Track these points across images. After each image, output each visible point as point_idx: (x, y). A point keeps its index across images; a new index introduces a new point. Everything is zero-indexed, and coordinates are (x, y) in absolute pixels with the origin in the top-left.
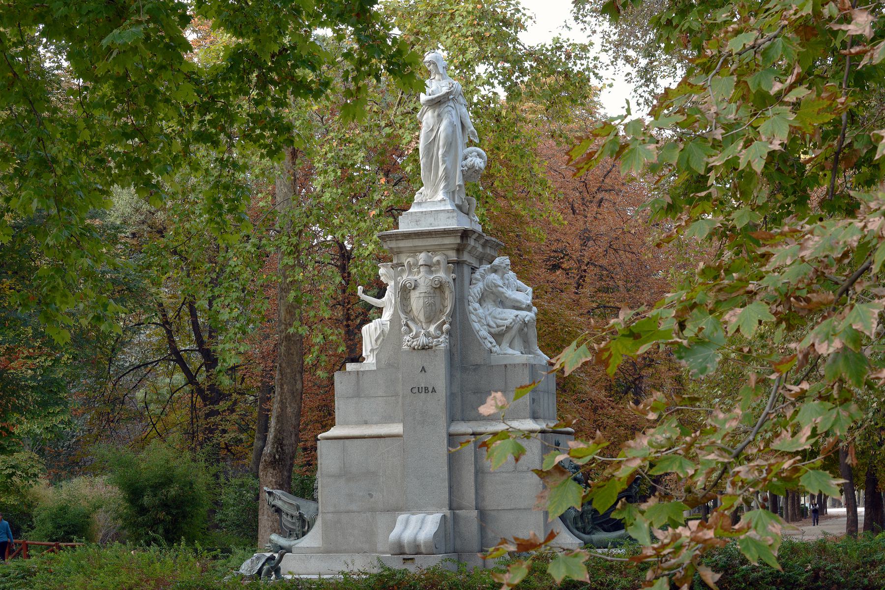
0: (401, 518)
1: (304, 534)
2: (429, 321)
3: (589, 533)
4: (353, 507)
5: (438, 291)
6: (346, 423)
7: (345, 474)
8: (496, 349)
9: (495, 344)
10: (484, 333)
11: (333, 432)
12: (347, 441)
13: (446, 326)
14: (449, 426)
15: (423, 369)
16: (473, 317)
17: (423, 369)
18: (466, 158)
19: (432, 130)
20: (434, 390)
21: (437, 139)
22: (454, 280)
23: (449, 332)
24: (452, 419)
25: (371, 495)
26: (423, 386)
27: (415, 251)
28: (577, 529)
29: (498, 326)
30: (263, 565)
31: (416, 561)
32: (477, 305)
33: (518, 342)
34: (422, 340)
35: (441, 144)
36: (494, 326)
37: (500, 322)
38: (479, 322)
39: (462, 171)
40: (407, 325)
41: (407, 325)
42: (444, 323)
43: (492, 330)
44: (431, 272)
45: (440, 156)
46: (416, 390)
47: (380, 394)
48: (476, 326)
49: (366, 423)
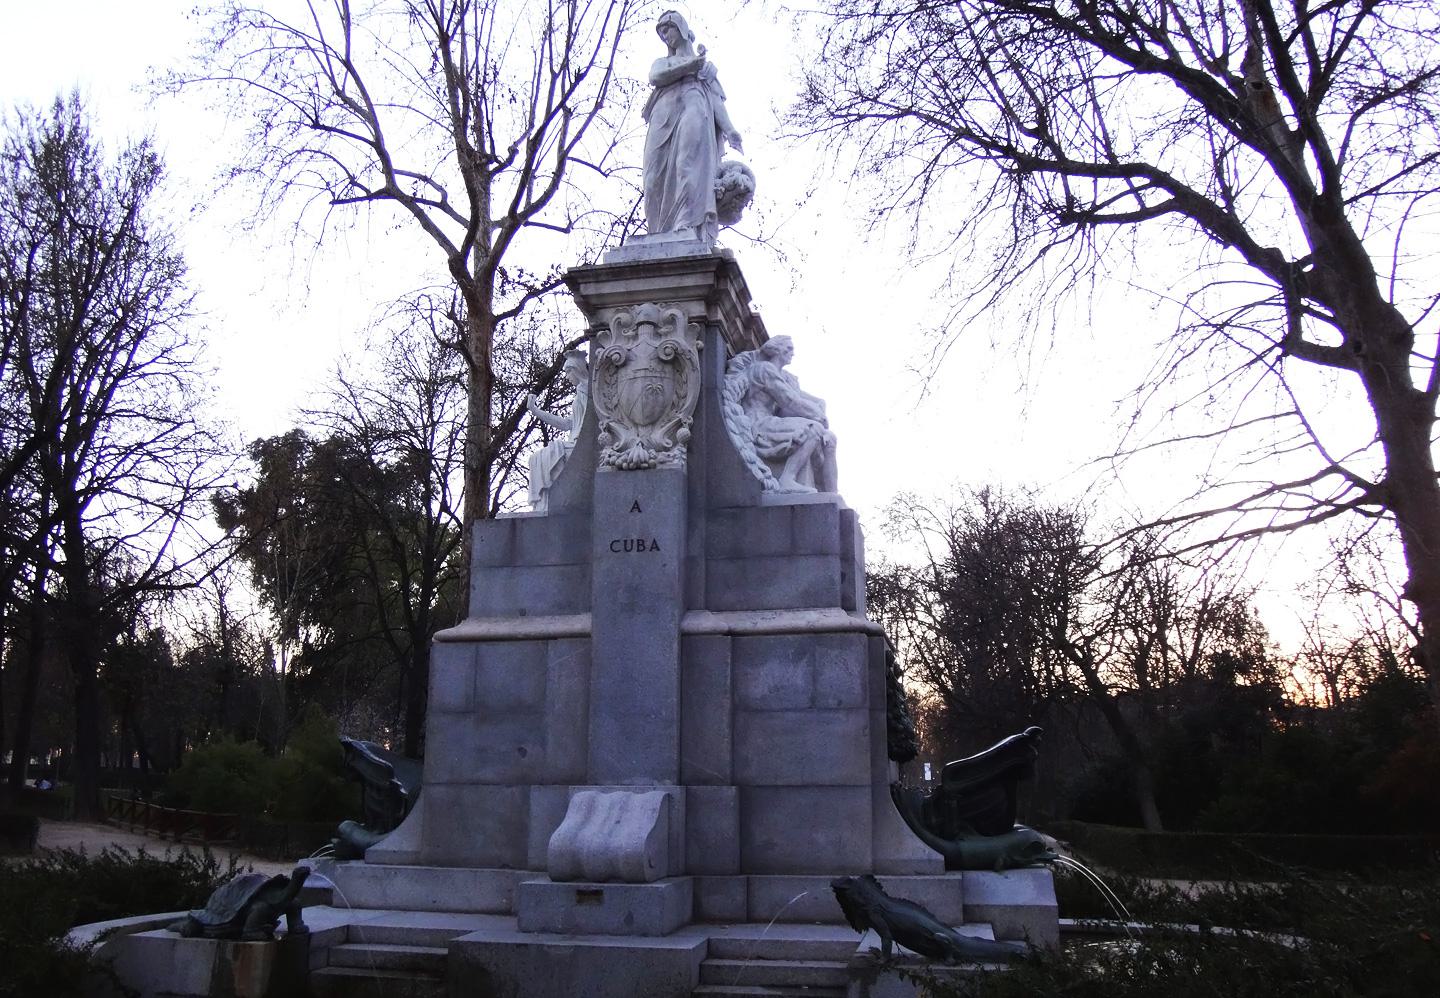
0: (580, 797)
1: (396, 823)
2: (652, 422)
3: (951, 838)
4: (488, 774)
5: (668, 368)
6: (487, 614)
7: (475, 708)
8: (772, 482)
9: (769, 473)
10: (748, 452)
11: (465, 628)
12: (484, 646)
13: (684, 431)
14: (682, 617)
15: (636, 507)
16: (731, 424)
17: (636, 507)
18: (721, 176)
19: (667, 126)
20: (655, 546)
21: (674, 141)
22: (700, 351)
23: (689, 443)
24: (689, 606)
25: (522, 752)
26: (635, 537)
27: (631, 300)
28: (930, 828)
29: (776, 443)
30: (252, 900)
31: (606, 896)
32: (739, 408)
33: (809, 474)
34: (637, 453)
35: (682, 144)
36: (769, 444)
37: (782, 436)
38: (742, 434)
39: (716, 191)
40: (609, 429)
41: (609, 429)
42: (679, 424)
43: (764, 452)
44: (658, 335)
45: (679, 165)
46: (619, 546)
47: (553, 560)
48: (737, 440)
49: (523, 613)
